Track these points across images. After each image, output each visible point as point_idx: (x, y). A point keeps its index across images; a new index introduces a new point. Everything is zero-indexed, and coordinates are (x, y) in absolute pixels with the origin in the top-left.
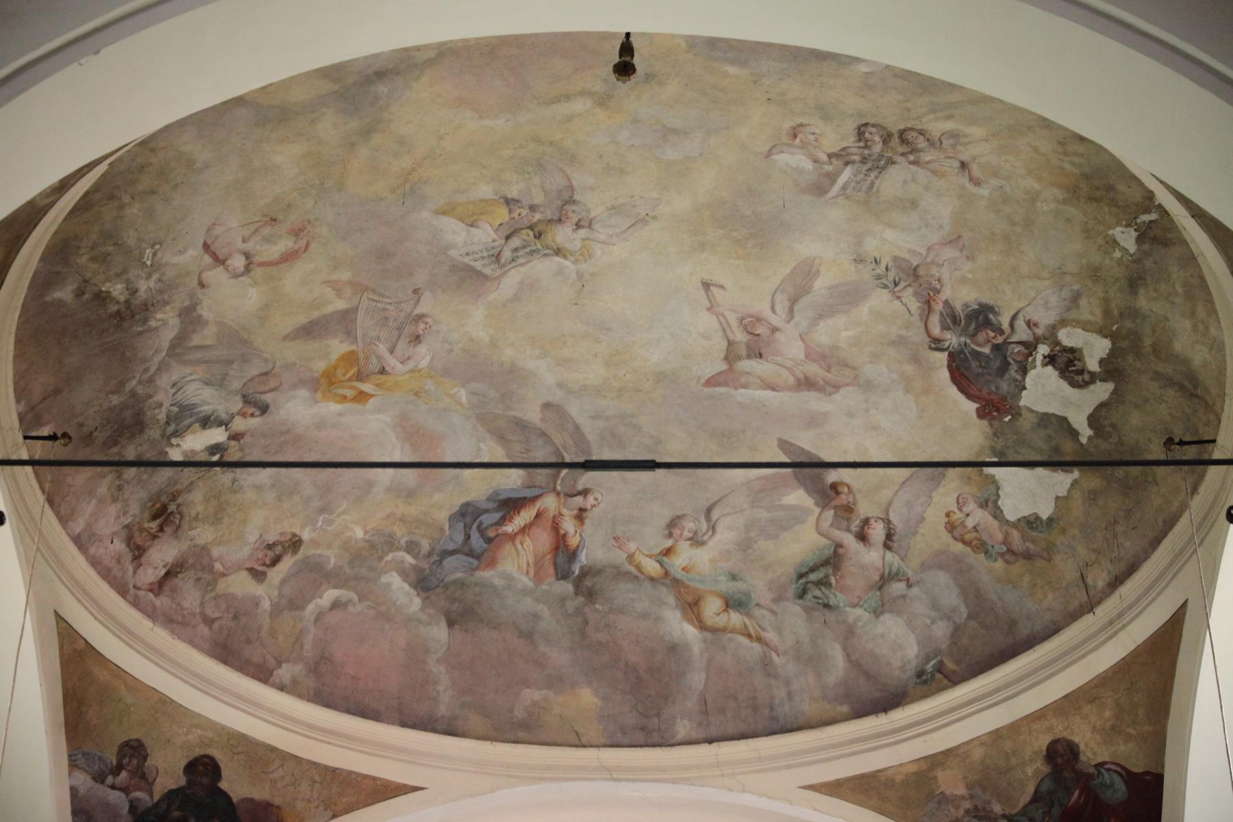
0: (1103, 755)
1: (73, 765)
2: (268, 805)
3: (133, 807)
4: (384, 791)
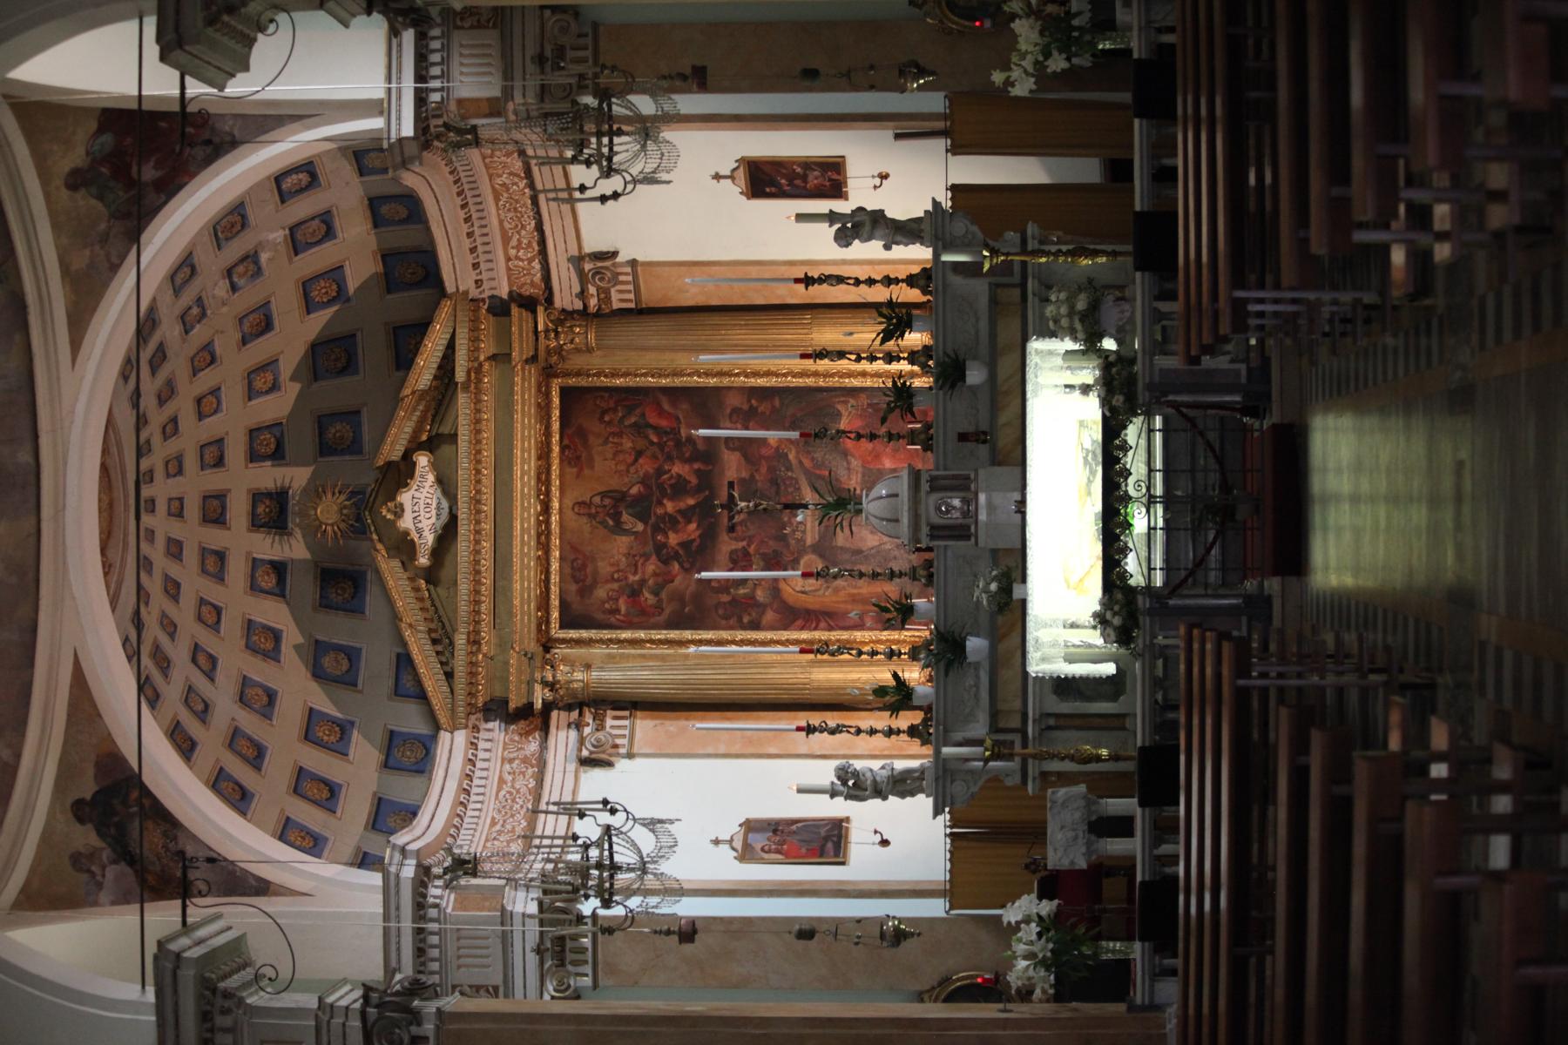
0: (80, 151)
1: (95, 904)
2: (97, 765)
3: (115, 862)
4: (79, 680)
